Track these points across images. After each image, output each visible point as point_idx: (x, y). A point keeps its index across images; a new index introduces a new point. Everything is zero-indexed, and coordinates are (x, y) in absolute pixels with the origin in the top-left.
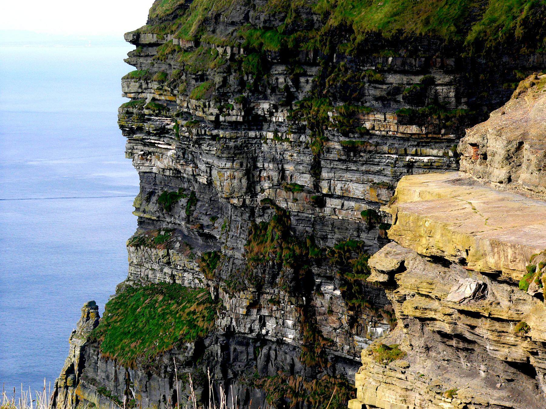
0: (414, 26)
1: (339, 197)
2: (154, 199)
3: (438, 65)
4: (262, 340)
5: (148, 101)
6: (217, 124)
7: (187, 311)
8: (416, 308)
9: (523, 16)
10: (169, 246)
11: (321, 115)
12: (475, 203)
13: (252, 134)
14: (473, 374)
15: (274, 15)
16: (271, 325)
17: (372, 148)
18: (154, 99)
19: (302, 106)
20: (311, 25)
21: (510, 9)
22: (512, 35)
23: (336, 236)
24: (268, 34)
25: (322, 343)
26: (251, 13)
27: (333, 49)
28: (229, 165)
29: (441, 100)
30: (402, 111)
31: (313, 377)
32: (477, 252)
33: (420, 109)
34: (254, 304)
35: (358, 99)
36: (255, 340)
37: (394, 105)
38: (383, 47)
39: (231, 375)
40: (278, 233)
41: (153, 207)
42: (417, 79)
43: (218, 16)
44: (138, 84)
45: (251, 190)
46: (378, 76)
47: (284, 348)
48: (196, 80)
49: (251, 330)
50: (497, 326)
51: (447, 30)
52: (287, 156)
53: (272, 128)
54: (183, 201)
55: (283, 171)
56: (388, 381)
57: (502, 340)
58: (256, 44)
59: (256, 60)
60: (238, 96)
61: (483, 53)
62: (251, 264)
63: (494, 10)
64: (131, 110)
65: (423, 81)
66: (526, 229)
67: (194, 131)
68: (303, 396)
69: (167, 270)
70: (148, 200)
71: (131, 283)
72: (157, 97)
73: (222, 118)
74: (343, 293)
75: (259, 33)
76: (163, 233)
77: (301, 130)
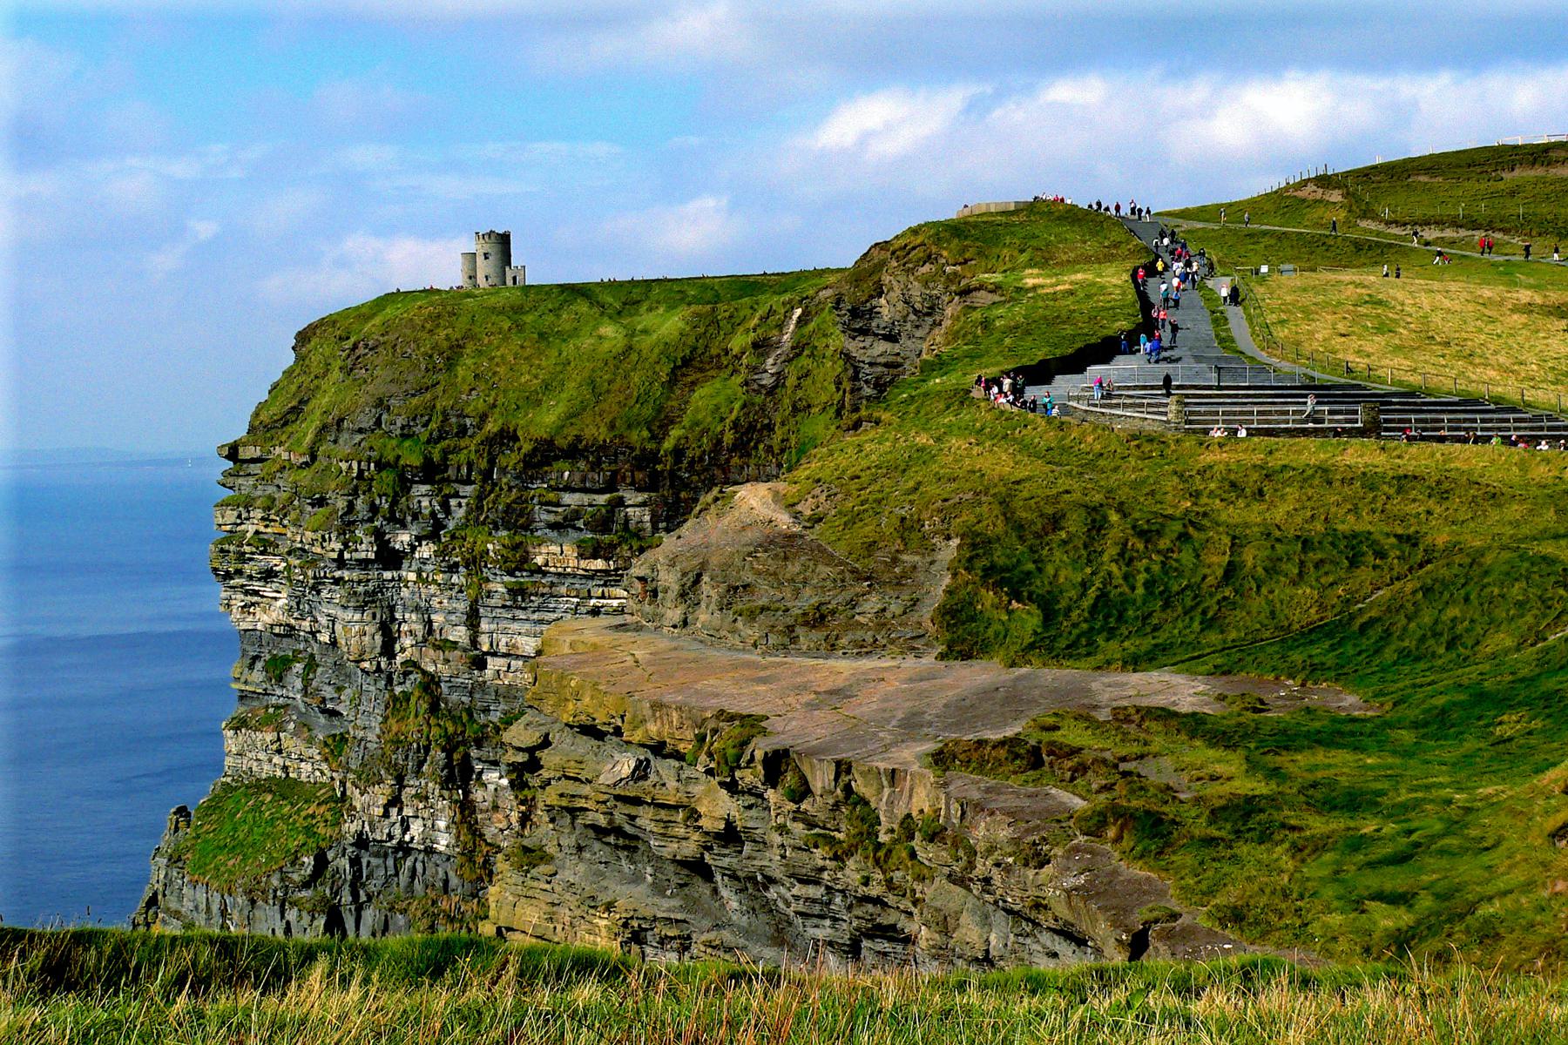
0: (596, 431)
1: (505, 655)
2: (259, 665)
3: (628, 480)
4: (404, 849)
5: (249, 535)
6: (341, 563)
7: (303, 814)
8: (562, 795)
9: (733, 417)
10: (280, 729)
11: (477, 549)
12: (639, 654)
13: (388, 575)
14: (637, 879)
15: (414, 419)
16: (416, 828)
17: (546, 590)
18: (257, 532)
19: (453, 537)
20: (462, 431)
21: (717, 408)
22: (720, 441)
23: (502, 707)
24: (407, 443)
25: (485, 849)
26: (384, 417)
27: (492, 462)
28: (357, 616)
29: (632, 525)
30: (583, 541)
31: (474, 895)
32: (635, 716)
33: (606, 538)
34: (395, 801)
35: (526, 527)
36: (396, 849)
37: (573, 534)
38: (557, 458)
39: (363, 898)
40: (425, 706)
41: (258, 676)
42: (602, 499)
43: (341, 420)
45: (388, 650)
46: (551, 496)
47: (435, 858)
48: (313, 505)
49: (390, 837)
50: (663, 815)
51: (638, 436)
52: (435, 602)
53: (414, 567)
54: (298, 667)
55: (430, 622)
56: (530, 893)
57: (670, 832)
58: (391, 458)
59: (391, 478)
60: (368, 525)
61: (685, 464)
62: (388, 749)
63: (697, 410)
64: (226, 547)
65: (609, 502)
66: (699, 686)
67: (310, 573)
68: (461, 921)
69: (277, 759)
70: (251, 667)
71: (229, 780)
72: (262, 529)
73: (347, 556)
74: (512, 783)
75: (394, 442)
76: (271, 710)
77: (453, 568)
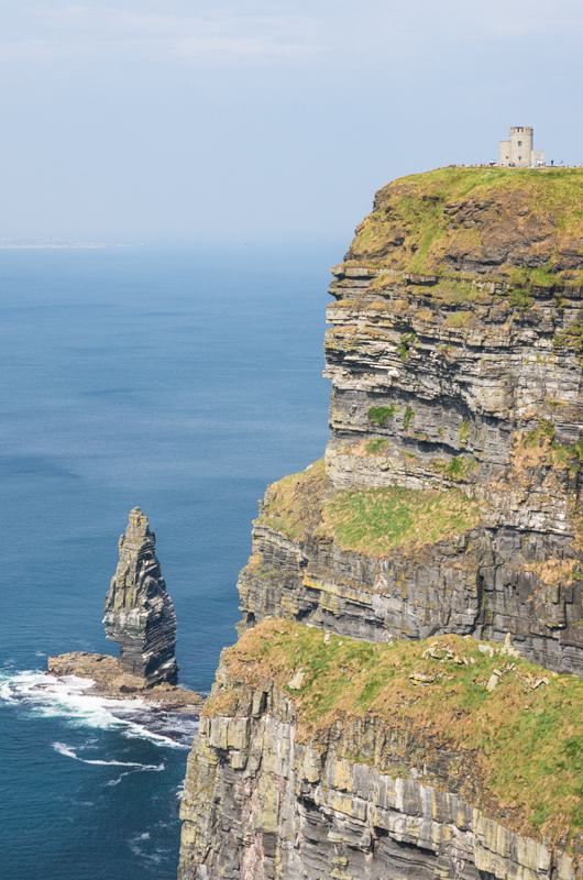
6: (480, 349)
13: (514, 357)
28: (493, 383)
52: (550, 375)
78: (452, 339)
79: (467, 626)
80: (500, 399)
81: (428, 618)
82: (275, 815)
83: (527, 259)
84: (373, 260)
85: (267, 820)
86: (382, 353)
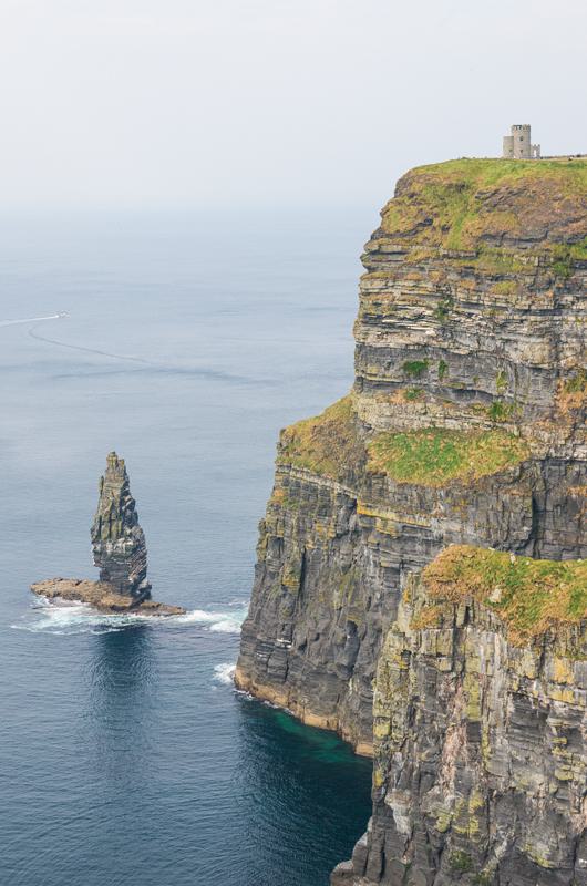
6: (526, 312)
13: (556, 318)
28: (540, 340)
44: (384, 283)
78: (498, 304)
79: (522, 541)
80: (546, 353)
81: (489, 536)
82: (479, 708)
83: (566, 237)
84: (406, 239)
85: (471, 711)
86: (420, 317)
